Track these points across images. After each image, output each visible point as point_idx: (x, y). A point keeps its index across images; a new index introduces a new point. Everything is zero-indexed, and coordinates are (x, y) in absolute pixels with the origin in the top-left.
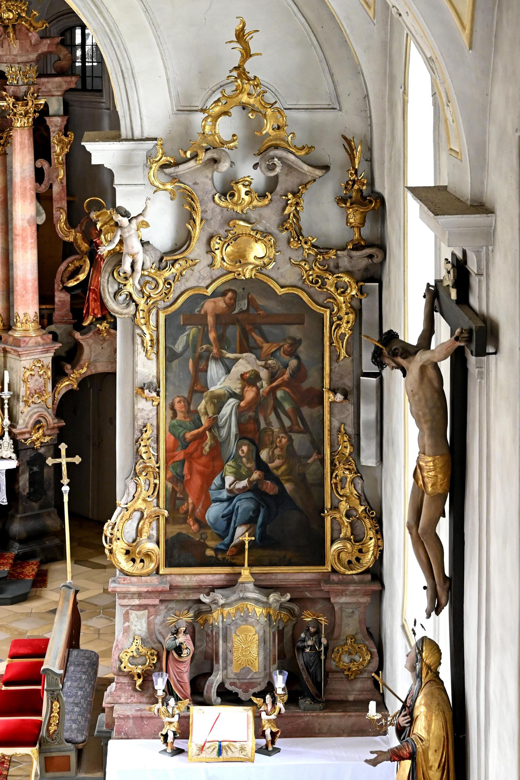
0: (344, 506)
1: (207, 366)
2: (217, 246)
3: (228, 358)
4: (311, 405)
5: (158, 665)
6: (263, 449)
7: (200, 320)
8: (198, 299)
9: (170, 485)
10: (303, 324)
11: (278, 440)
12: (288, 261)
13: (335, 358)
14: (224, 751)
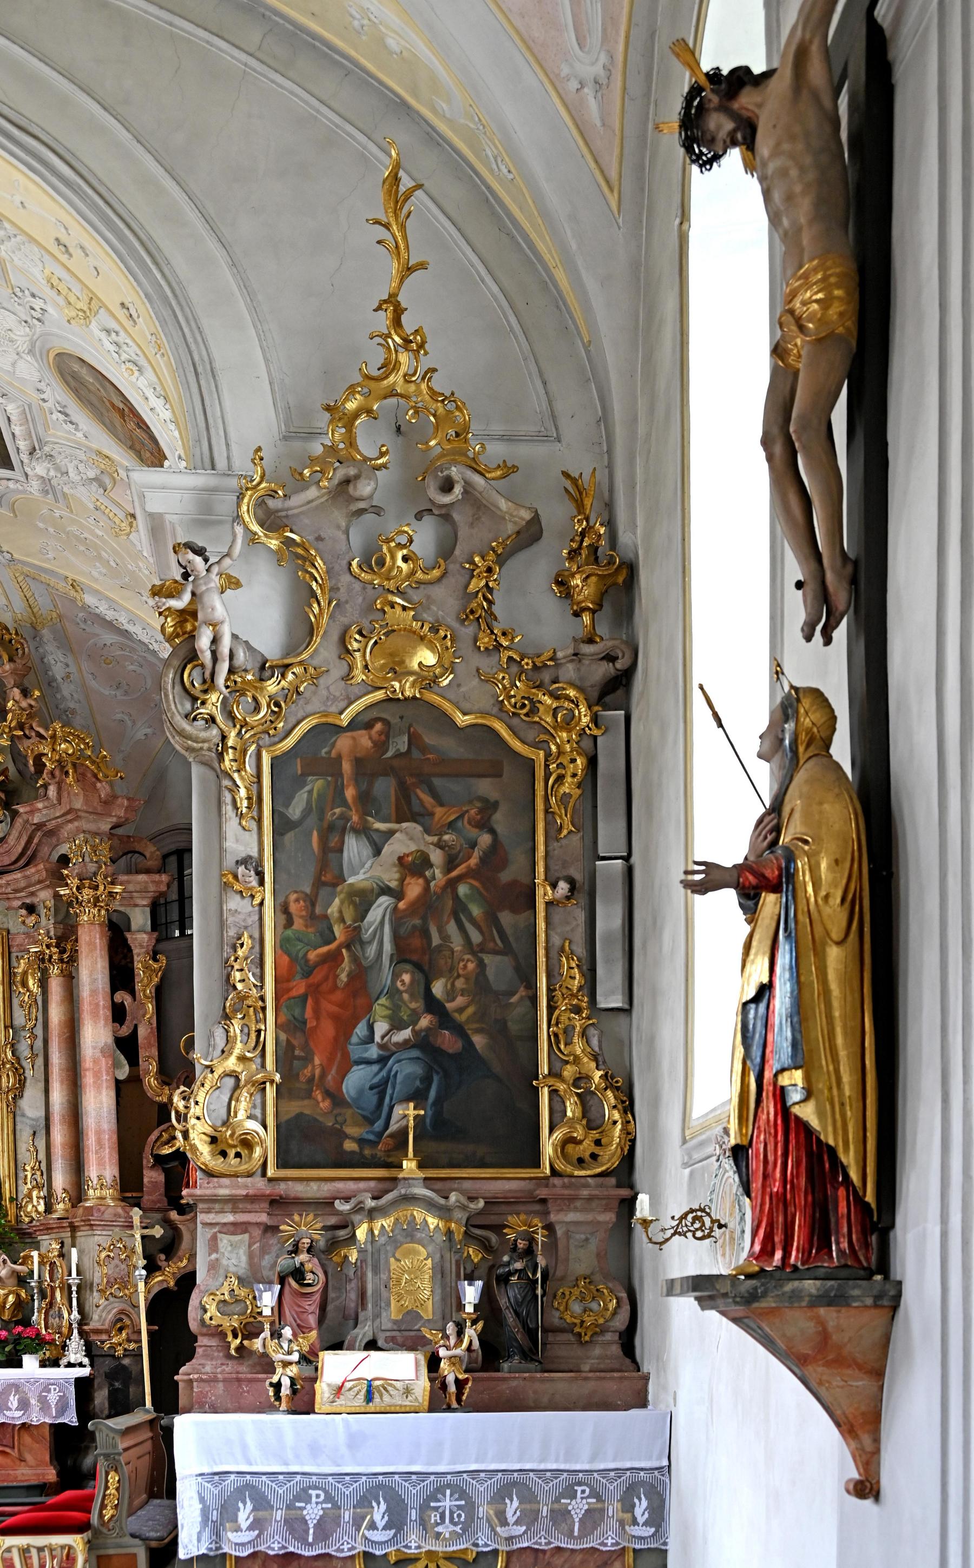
0: (569, 1072)
1: (343, 843)
2: (356, 645)
3: (377, 830)
4: (515, 910)
6: (437, 979)
7: (332, 767)
8: (326, 731)
9: (283, 1036)
10: (501, 776)
11: (461, 964)
12: (475, 673)
13: (553, 833)
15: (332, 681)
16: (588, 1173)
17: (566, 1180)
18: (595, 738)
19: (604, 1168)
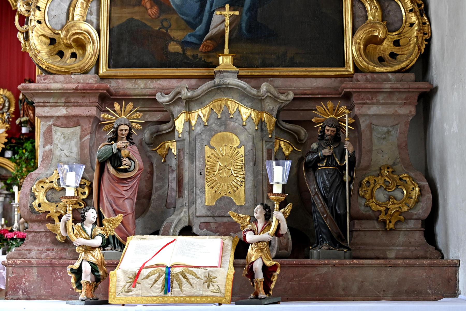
5: (89, 202)
14: (175, 284)
16: (389, 69)
17: (369, 76)
19: (403, 65)
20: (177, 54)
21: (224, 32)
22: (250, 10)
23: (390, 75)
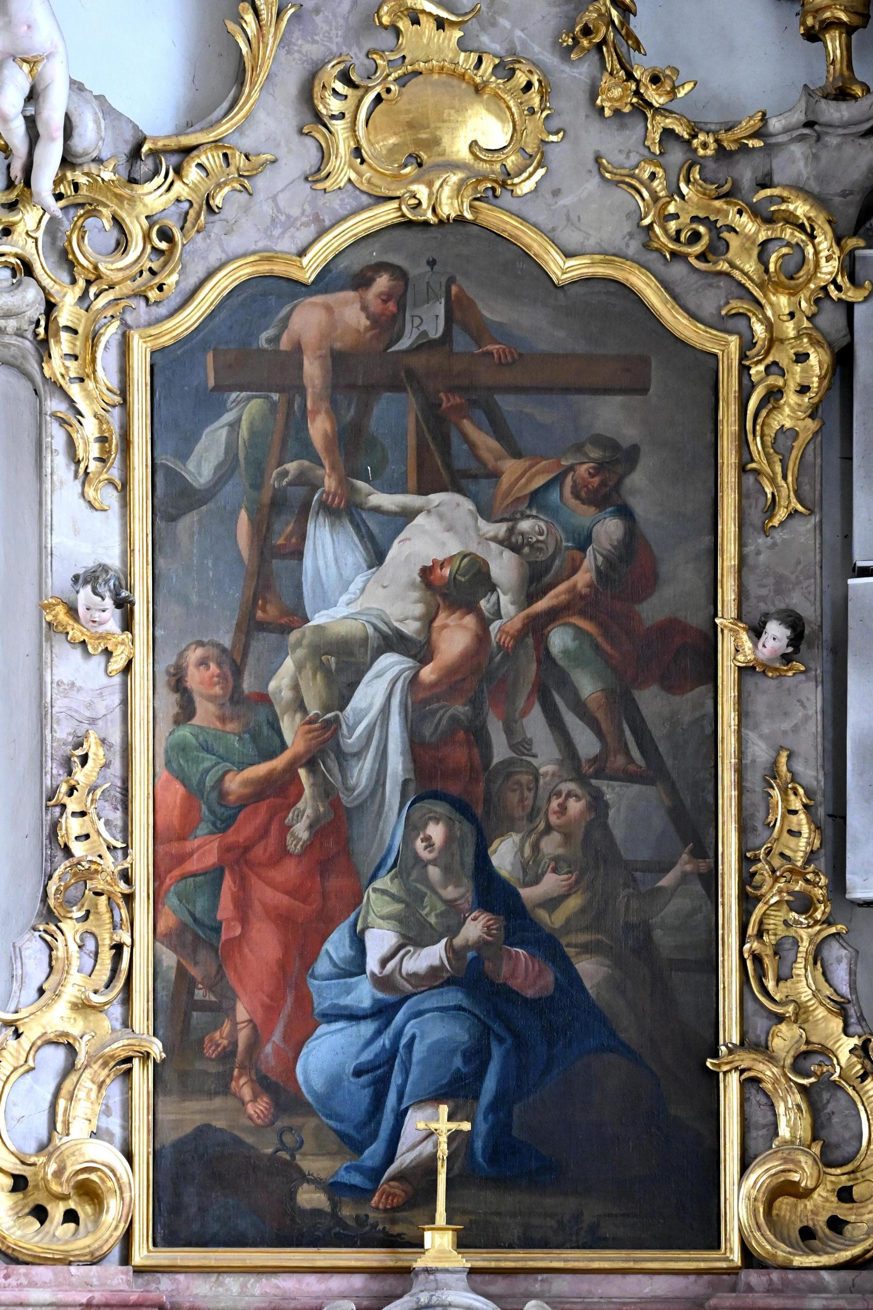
0: (784, 1039)
1: (303, 537)
2: (336, 105)
3: (377, 510)
4: (672, 684)
6: (502, 834)
7: (278, 373)
8: (267, 294)
9: (170, 959)
10: (644, 391)
11: (555, 804)
12: (591, 165)
13: (755, 516)
15: (282, 184)
16: (824, 1260)
17: (775, 1275)
18: (850, 307)
19: (857, 1250)
20: (317, 1213)
21: (433, 1158)
22: (494, 1107)
23: (825, 1274)
